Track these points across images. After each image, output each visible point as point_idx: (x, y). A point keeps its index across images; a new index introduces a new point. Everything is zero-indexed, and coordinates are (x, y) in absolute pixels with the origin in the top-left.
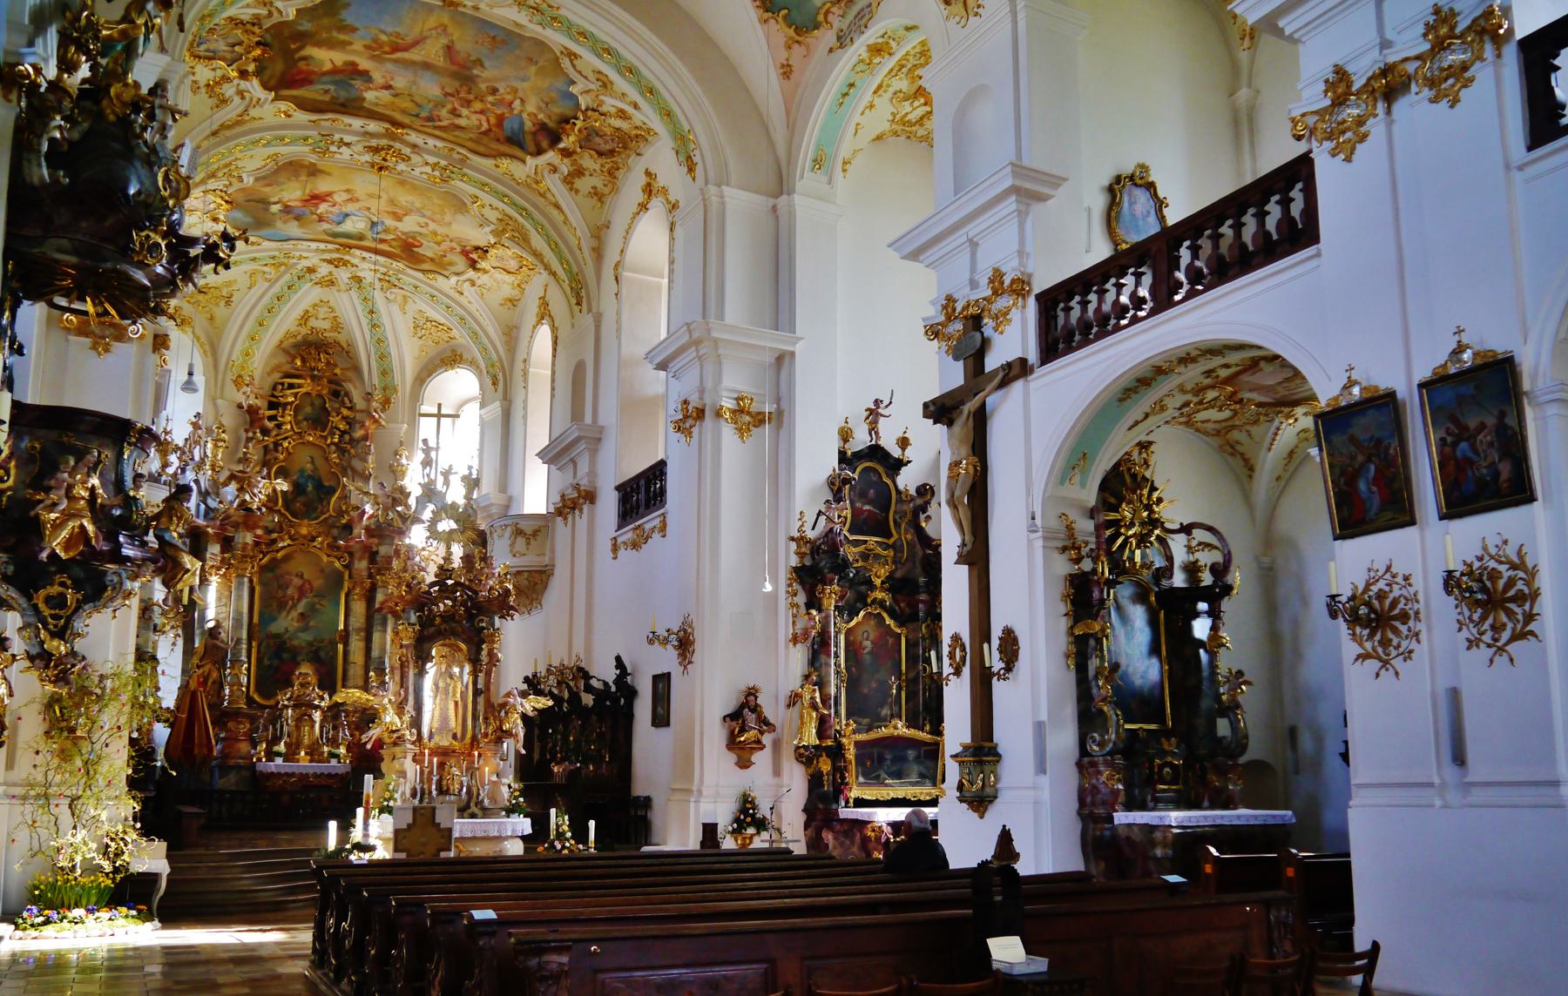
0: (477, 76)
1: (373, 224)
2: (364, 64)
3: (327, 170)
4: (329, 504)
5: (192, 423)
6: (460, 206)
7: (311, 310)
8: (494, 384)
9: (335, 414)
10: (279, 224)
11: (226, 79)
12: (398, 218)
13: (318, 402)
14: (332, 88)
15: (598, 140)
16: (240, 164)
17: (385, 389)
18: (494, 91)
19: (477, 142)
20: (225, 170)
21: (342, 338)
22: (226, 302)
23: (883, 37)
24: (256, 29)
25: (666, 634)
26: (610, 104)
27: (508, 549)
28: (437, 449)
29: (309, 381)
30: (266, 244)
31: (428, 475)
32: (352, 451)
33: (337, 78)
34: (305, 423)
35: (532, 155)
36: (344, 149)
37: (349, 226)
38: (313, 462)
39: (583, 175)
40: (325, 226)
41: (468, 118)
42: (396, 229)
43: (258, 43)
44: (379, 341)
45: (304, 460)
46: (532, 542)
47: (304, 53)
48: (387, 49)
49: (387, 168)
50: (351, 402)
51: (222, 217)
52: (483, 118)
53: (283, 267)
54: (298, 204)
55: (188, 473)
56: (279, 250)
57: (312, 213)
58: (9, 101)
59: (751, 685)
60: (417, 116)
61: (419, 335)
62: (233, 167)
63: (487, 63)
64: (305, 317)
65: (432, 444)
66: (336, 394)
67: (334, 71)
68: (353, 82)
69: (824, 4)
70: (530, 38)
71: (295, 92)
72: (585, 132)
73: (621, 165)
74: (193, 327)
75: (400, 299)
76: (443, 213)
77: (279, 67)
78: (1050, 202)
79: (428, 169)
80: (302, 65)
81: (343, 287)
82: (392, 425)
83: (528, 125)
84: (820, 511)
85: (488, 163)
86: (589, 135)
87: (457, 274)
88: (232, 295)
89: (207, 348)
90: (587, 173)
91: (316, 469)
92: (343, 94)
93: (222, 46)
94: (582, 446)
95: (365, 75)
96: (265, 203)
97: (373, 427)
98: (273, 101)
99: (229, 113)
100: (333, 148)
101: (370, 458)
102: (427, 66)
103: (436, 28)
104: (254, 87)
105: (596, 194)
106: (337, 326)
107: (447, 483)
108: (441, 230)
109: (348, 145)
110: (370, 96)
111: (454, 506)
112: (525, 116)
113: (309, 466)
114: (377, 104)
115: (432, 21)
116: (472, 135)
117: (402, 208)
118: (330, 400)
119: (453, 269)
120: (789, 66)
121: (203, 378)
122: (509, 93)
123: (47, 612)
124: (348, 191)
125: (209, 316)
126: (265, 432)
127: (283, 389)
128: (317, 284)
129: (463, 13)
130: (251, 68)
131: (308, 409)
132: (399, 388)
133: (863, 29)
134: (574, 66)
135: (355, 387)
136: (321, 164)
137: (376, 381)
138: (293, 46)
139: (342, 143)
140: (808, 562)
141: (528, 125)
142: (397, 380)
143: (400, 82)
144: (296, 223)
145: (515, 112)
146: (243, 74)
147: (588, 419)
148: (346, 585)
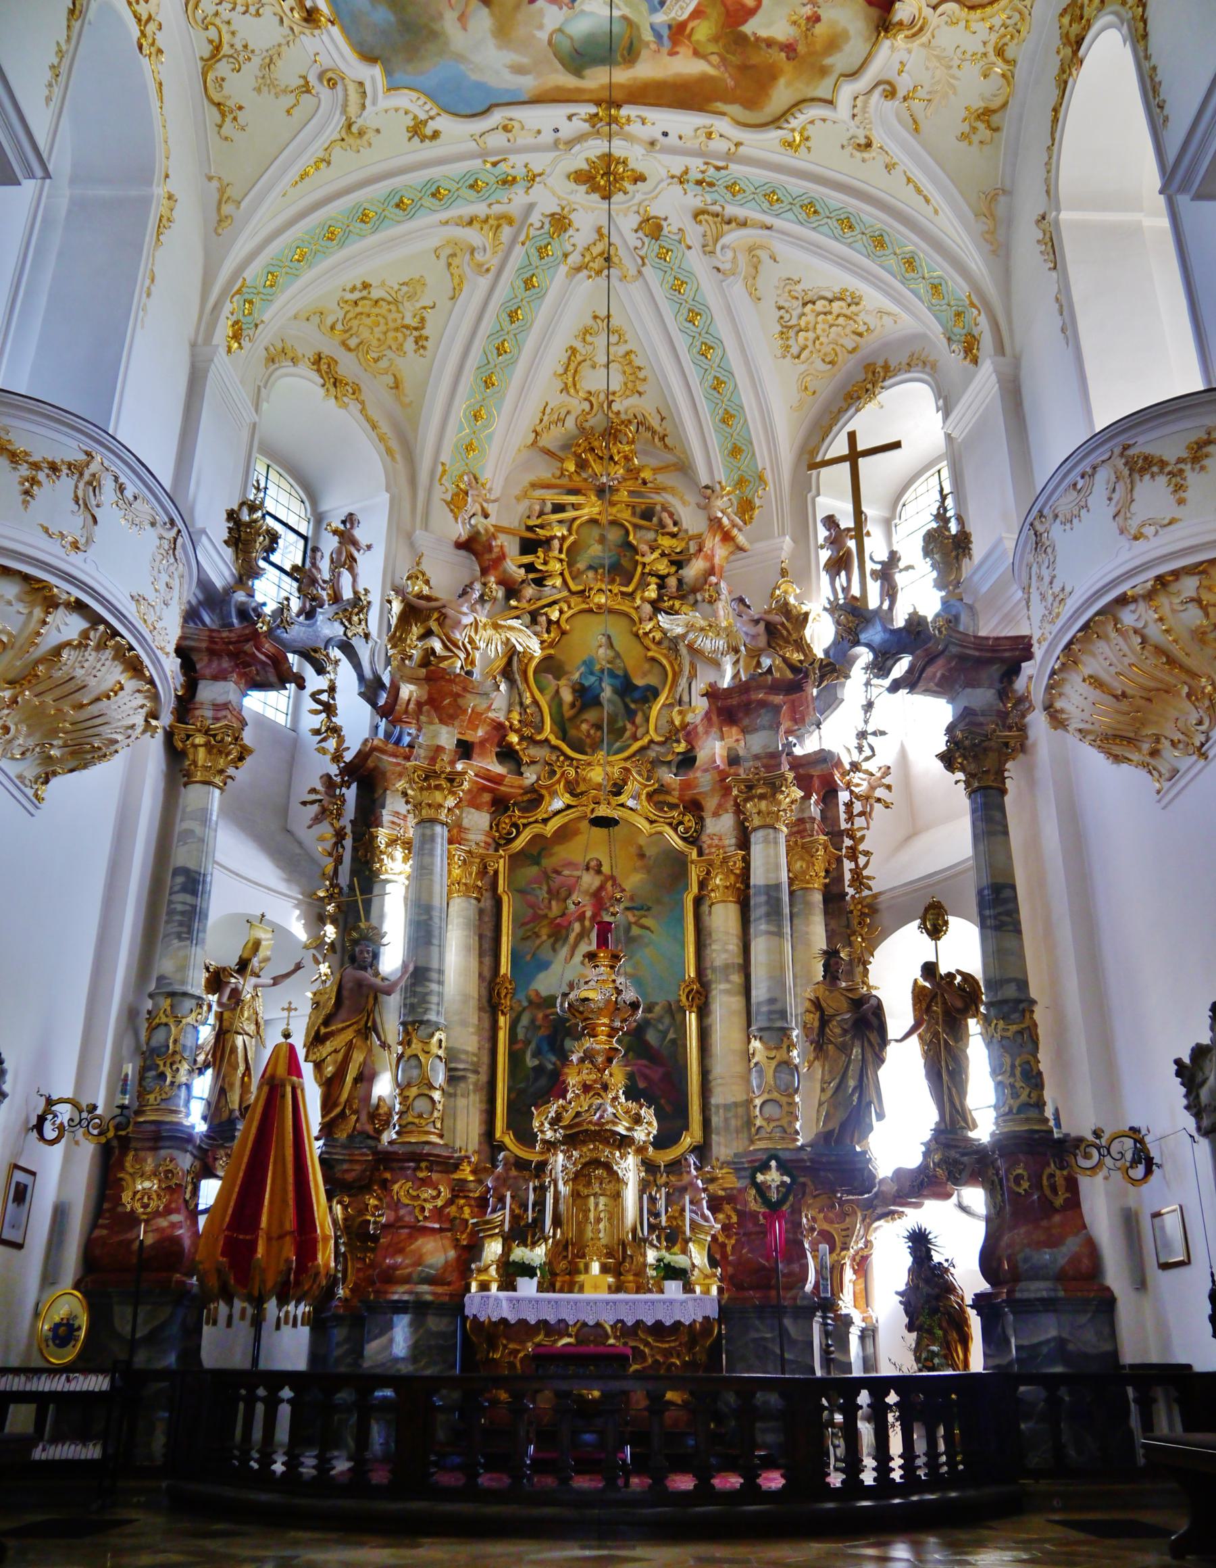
4: (647, 720)
7: (578, 345)
13: (614, 535)
17: (740, 483)
21: (645, 405)
22: (416, 343)
29: (594, 498)
31: (846, 590)
34: (591, 574)
38: (611, 645)
44: (717, 386)
50: (675, 524)
53: (506, 232)
61: (795, 350)
64: (573, 364)
65: (847, 522)
74: (362, 403)
82: (761, 546)
88: (423, 320)
89: (394, 444)
91: (618, 655)
106: (635, 378)
111: (916, 624)
113: (601, 651)
118: (636, 526)
119: (840, 61)
121: (387, 496)
125: (390, 380)
127: (541, 514)
128: (578, 269)
131: (596, 550)
132: (768, 475)
135: (684, 503)
137: (721, 475)
142: (763, 459)
148: (694, 874)
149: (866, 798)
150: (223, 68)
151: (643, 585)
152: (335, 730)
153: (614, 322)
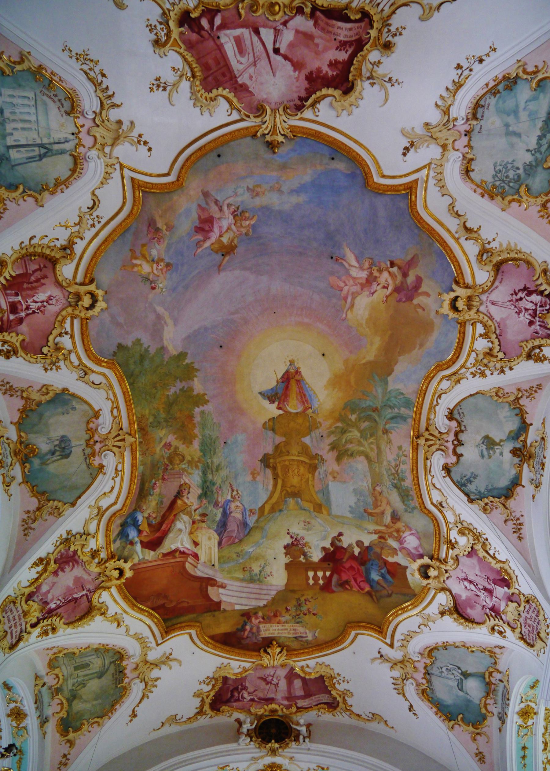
23: (522, 702)
69: (481, 700)
120: (480, 753)
133: (507, 702)
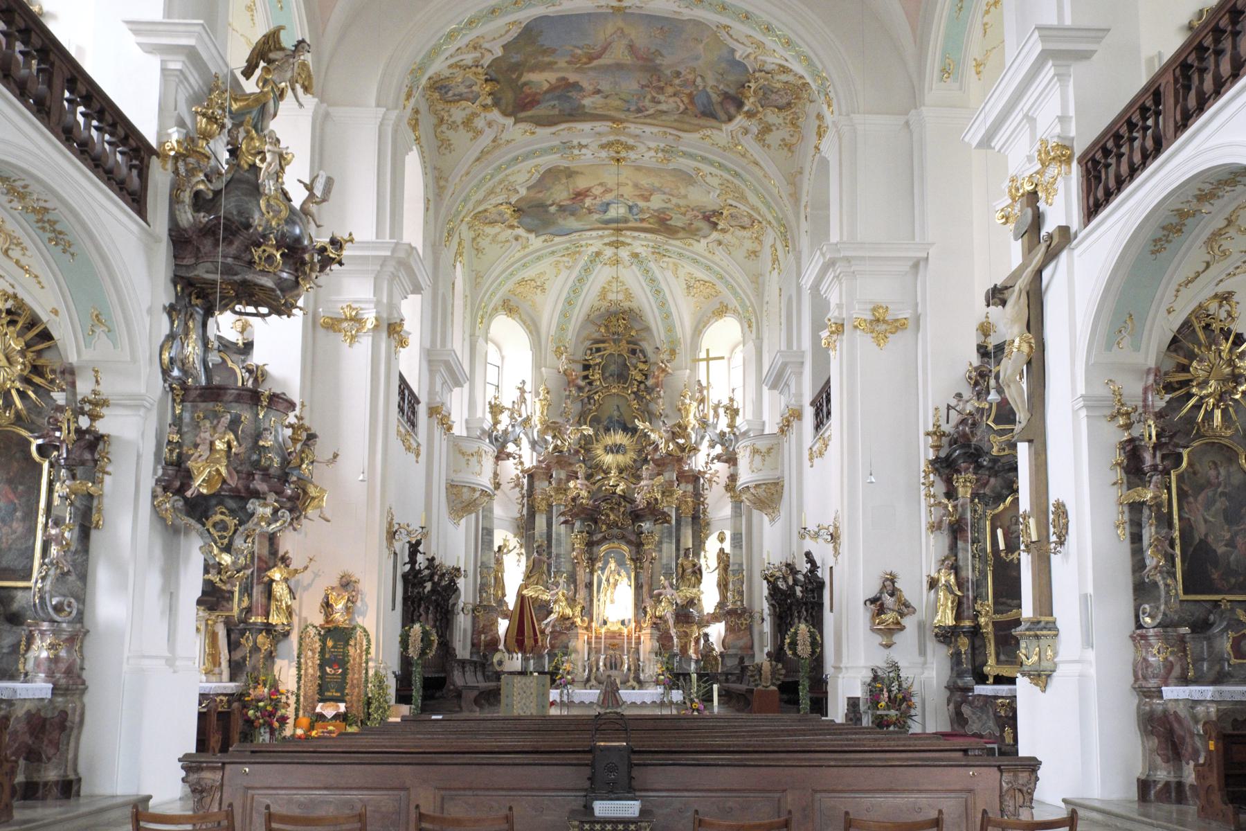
0: (661, 65)
1: (630, 208)
2: (572, 77)
3: (579, 170)
5: (519, 388)
6: (687, 178)
8: (750, 326)
9: (632, 368)
10: (561, 221)
11: (475, 115)
12: (647, 199)
13: (620, 360)
14: (556, 102)
15: (774, 97)
16: (511, 179)
18: (678, 74)
19: (682, 122)
20: (502, 186)
21: (634, 305)
24: (480, 70)
25: (817, 530)
26: (772, 61)
27: (748, 466)
28: (708, 388)
30: (557, 239)
32: (648, 397)
33: (557, 93)
35: (725, 122)
36: (584, 151)
37: (612, 213)
39: (771, 130)
40: (596, 216)
41: (666, 102)
42: (649, 208)
43: (486, 80)
44: (663, 304)
45: (611, 410)
46: (767, 458)
47: (524, 79)
48: (584, 60)
49: (624, 159)
51: (516, 224)
52: (677, 99)
54: (569, 202)
55: (517, 428)
56: (570, 241)
57: (582, 208)
58: (166, 170)
59: (889, 572)
60: (628, 110)
62: (507, 183)
63: (664, 52)
64: (603, 294)
65: (704, 383)
66: (634, 352)
67: (552, 89)
68: (570, 94)
70: (690, 20)
71: (529, 113)
72: (761, 93)
73: (800, 115)
75: (671, 265)
76: (678, 188)
77: (509, 97)
78: (1095, 57)
79: (652, 153)
80: (526, 89)
81: (629, 264)
82: (678, 372)
83: (715, 98)
84: (949, 406)
85: (696, 136)
86: (765, 94)
87: (705, 237)
89: (532, 328)
90: (774, 128)
91: (621, 414)
92: (567, 106)
93: (463, 89)
94: (789, 371)
95: (576, 86)
96: (542, 207)
97: (662, 375)
98: (515, 123)
99: (485, 140)
100: (576, 152)
101: (660, 401)
102: (619, 67)
103: (615, 32)
104: (495, 114)
105: (786, 145)
106: (629, 296)
107: (717, 415)
108: (682, 202)
109: (585, 146)
110: (587, 102)
111: (723, 434)
112: (708, 89)
113: (616, 413)
114: (596, 108)
115: (610, 28)
116: (676, 117)
117: (646, 190)
119: (701, 233)
122: (689, 73)
123: (216, 534)
124: (601, 184)
126: (580, 389)
129: (632, 14)
130: (489, 101)
131: (613, 368)
132: (682, 340)
134: (731, 36)
135: (649, 345)
136: (573, 165)
137: (663, 337)
138: (514, 76)
139: (581, 146)
140: (943, 454)
141: (715, 98)
142: (680, 335)
143: (605, 86)
144: (572, 218)
145: (700, 88)
146: (485, 107)
147: (795, 348)
149: (710, 481)
150: (479, 239)
151: (631, 385)
152: (521, 463)
153: (621, 279)
